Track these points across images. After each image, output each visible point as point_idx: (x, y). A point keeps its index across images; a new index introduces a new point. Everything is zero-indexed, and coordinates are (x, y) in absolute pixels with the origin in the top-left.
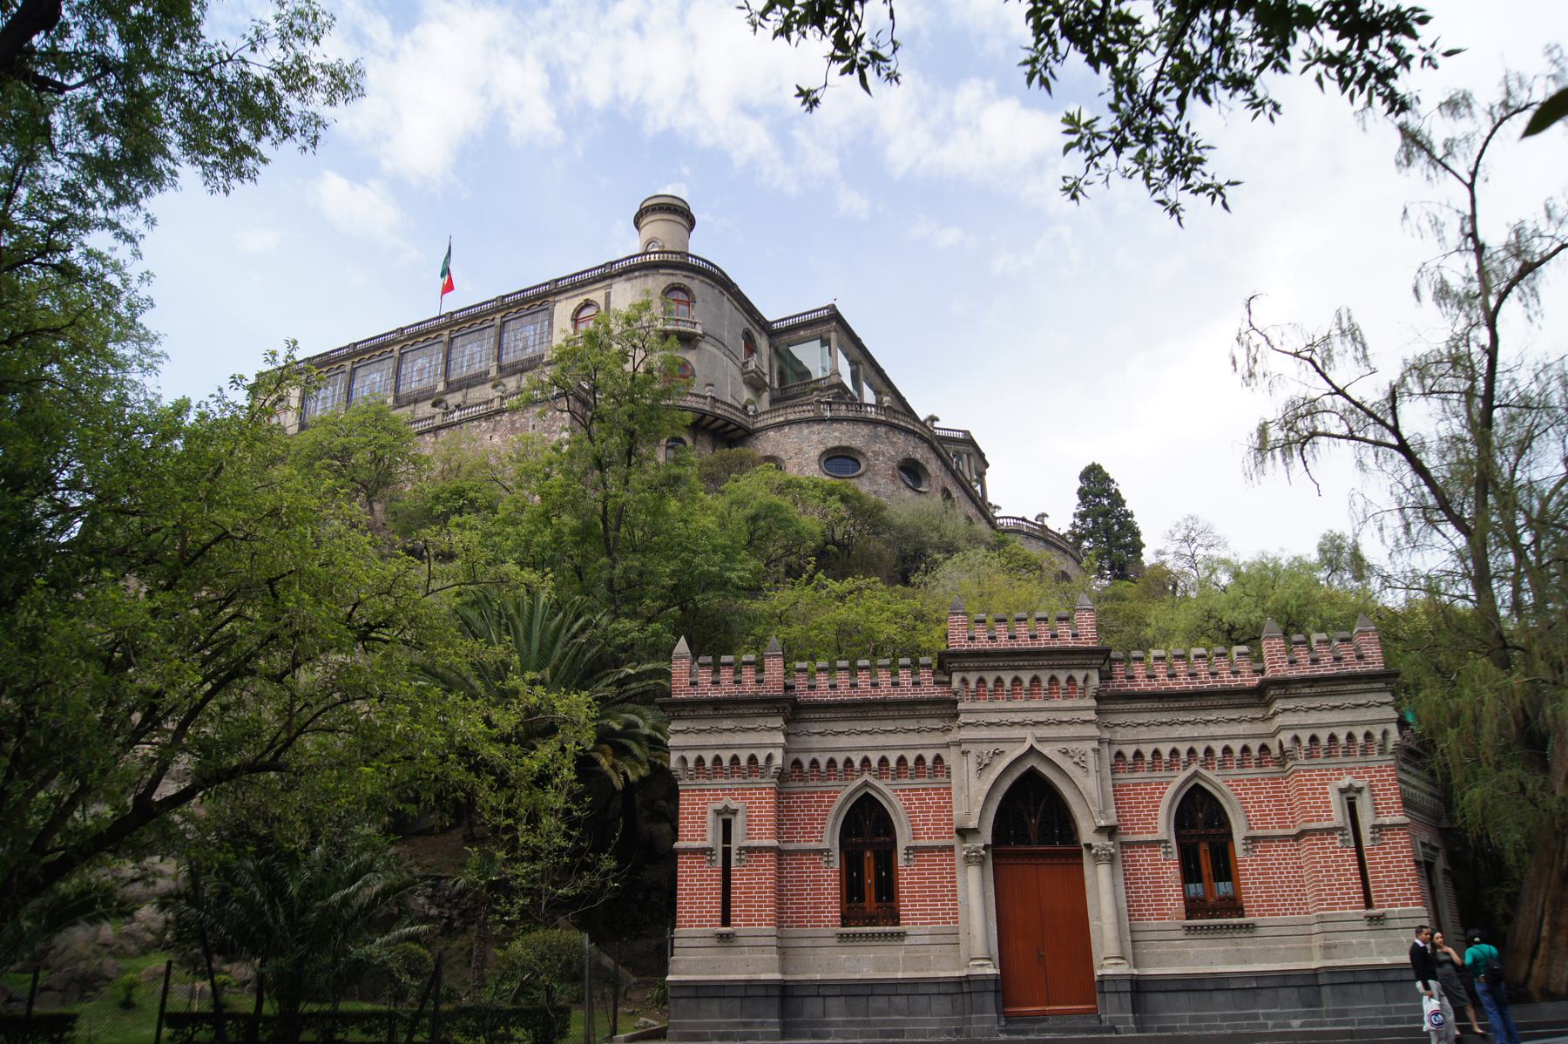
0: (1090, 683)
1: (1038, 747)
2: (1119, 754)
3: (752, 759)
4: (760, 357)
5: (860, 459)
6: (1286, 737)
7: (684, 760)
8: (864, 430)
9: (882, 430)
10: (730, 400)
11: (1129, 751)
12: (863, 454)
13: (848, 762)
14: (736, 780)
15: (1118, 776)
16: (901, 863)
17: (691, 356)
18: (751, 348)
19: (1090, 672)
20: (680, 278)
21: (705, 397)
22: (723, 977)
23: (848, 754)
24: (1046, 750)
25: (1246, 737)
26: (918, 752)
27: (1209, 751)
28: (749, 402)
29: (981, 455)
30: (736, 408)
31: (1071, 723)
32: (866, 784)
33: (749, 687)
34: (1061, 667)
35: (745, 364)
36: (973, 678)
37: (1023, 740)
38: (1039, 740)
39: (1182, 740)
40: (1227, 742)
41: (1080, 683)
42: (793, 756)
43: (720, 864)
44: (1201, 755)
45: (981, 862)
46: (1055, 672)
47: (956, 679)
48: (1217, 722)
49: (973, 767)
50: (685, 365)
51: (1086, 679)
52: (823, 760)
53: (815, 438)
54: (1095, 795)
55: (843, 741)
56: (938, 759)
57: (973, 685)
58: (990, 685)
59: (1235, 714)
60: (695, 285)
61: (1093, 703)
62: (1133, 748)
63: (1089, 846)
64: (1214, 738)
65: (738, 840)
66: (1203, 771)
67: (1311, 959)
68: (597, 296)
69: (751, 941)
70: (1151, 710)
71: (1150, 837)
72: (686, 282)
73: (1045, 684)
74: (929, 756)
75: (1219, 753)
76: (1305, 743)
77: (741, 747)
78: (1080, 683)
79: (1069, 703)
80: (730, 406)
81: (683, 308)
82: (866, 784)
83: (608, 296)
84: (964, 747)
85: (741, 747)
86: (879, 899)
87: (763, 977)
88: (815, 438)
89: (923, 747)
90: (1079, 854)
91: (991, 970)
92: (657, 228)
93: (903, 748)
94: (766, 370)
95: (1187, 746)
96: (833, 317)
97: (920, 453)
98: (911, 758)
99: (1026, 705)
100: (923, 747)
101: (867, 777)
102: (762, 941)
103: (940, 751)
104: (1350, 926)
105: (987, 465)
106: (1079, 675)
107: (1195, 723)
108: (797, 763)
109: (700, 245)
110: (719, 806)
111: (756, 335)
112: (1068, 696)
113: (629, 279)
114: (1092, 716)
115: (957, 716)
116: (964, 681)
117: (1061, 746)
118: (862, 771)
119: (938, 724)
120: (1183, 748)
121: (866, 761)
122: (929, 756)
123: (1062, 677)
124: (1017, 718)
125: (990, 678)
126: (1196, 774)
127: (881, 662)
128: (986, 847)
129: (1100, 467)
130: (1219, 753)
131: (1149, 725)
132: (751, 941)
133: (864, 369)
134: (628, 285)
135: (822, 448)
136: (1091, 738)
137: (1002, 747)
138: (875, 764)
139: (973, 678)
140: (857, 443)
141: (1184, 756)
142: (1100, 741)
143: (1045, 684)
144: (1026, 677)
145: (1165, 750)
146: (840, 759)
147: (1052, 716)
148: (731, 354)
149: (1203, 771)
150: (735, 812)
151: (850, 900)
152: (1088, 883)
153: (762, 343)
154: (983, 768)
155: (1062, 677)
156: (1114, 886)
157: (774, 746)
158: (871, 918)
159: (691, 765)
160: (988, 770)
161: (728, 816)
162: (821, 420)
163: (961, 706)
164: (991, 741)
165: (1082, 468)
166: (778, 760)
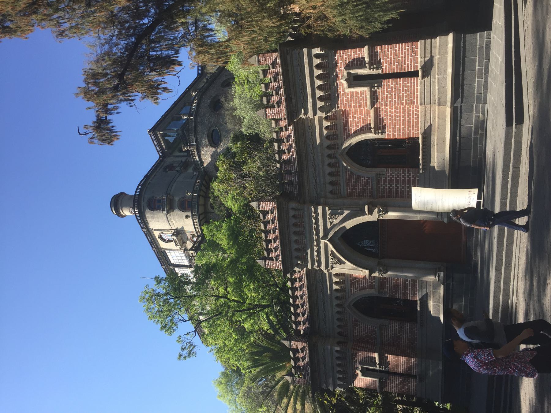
2: (331, 192)
5: (212, 129)
8: (200, 128)
9: (199, 119)
11: (329, 188)
12: (210, 128)
18: (171, 167)
41: (296, 213)
51: (293, 209)
68: (157, 234)
72: (146, 201)
78: (296, 213)
83: (156, 230)
94: (180, 159)
104: (427, 88)
106: (292, 213)
109: (131, 191)
113: (148, 223)
137: (330, 252)
145: (328, 170)
153: (169, 160)
157: (332, 349)
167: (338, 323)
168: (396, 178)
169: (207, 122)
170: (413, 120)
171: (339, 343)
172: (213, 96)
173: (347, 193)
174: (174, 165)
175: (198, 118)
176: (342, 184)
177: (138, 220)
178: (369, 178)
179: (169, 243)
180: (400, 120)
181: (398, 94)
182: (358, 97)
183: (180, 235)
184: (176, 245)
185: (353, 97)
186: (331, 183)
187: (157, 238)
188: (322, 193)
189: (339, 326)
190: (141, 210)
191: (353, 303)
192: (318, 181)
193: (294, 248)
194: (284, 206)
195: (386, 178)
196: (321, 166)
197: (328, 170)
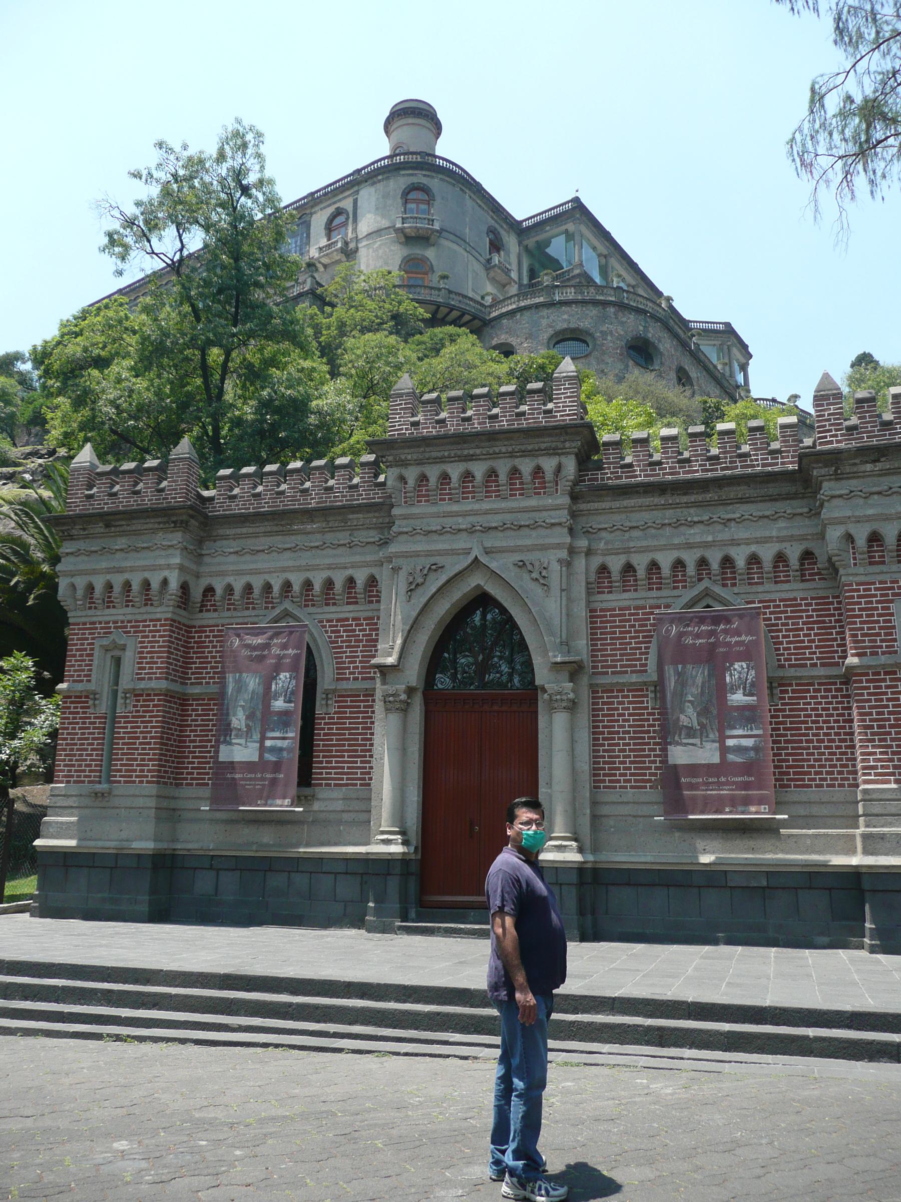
0: (563, 473)
1: (483, 559)
2: (603, 569)
4: (508, 254)
5: (588, 339)
6: (834, 534)
7: (73, 587)
8: (593, 311)
11: (616, 564)
12: (591, 335)
15: (592, 598)
17: (430, 253)
18: (496, 246)
19: (563, 459)
20: (420, 178)
21: (439, 289)
22: (92, 844)
23: (267, 577)
24: (493, 565)
25: (780, 540)
27: (727, 562)
28: (487, 294)
29: (745, 347)
31: (534, 526)
34: (525, 454)
35: (489, 261)
36: (411, 474)
37: (468, 551)
38: (487, 552)
39: (689, 546)
40: (753, 548)
41: (549, 476)
45: (405, 709)
46: (517, 462)
49: (403, 587)
50: (424, 260)
51: (559, 469)
53: (544, 322)
54: (556, 622)
55: (262, 562)
56: (372, 582)
57: (411, 482)
59: (767, 509)
60: (435, 183)
61: (566, 500)
64: (734, 543)
65: (125, 682)
67: (852, 851)
70: (650, 508)
71: (634, 678)
72: (425, 181)
75: (741, 563)
76: (861, 541)
77: (132, 569)
78: (549, 476)
79: (533, 502)
80: (471, 299)
81: (423, 207)
83: (355, 202)
84: (396, 562)
85: (132, 569)
87: (135, 845)
88: (544, 322)
92: (407, 132)
93: (330, 567)
94: (514, 266)
95: (697, 554)
96: (577, 210)
97: (654, 332)
98: (339, 580)
99: (476, 507)
100: (354, 566)
101: (287, 605)
105: (751, 356)
106: (549, 464)
107: (710, 523)
109: (446, 148)
110: (105, 642)
111: (503, 233)
113: (374, 184)
114: (563, 516)
116: (402, 479)
120: (690, 558)
121: (287, 586)
122: (361, 577)
123: (526, 466)
124: (463, 523)
125: (433, 473)
126: (707, 593)
128: (410, 691)
129: (870, 355)
131: (645, 528)
133: (614, 262)
134: (372, 190)
135: (551, 331)
136: (558, 546)
137: (440, 560)
139: (411, 474)
140: (585, 324)
141: (691, 570)
142: (572, 551)
144: (479, 470)
145: (665, 560)
149: (717, 589)
152: (541, 736)
153: (511, 241)
154: (413, 588)
155: (526, 466)
156: (573, 741)
157: (169, 567)
160: (420, 590)
161: (117, 653)
162: (551, 305)
163: (395, 511)
164: (429, 554)
165: (853, 358)
167: (238, 586)
168: (649, 732)
169: (604, 329)
170: (810, 773)
171: (184, 588)
172: (661, 347)
173: (602, 610)
174: (502, 253)
175: (612, 310)
176: (626, 595)
177: (376, 162)
178: (646, 665)
179: (323, 232)
180: (807, 741)
181: (890, 733)
182: (879, 635)
183: (344, 259)
184: (321, 249)
185: (878, 622)
186: (629, 568)
187: (336, 206)
188: (602, 545)
189: (229, 589)
190: (404, 169)
192: (636, 533)
193: (449, 471)
194: (567, 445)
195: (647, 708)
196: (676, 541)
197: (665, 560)
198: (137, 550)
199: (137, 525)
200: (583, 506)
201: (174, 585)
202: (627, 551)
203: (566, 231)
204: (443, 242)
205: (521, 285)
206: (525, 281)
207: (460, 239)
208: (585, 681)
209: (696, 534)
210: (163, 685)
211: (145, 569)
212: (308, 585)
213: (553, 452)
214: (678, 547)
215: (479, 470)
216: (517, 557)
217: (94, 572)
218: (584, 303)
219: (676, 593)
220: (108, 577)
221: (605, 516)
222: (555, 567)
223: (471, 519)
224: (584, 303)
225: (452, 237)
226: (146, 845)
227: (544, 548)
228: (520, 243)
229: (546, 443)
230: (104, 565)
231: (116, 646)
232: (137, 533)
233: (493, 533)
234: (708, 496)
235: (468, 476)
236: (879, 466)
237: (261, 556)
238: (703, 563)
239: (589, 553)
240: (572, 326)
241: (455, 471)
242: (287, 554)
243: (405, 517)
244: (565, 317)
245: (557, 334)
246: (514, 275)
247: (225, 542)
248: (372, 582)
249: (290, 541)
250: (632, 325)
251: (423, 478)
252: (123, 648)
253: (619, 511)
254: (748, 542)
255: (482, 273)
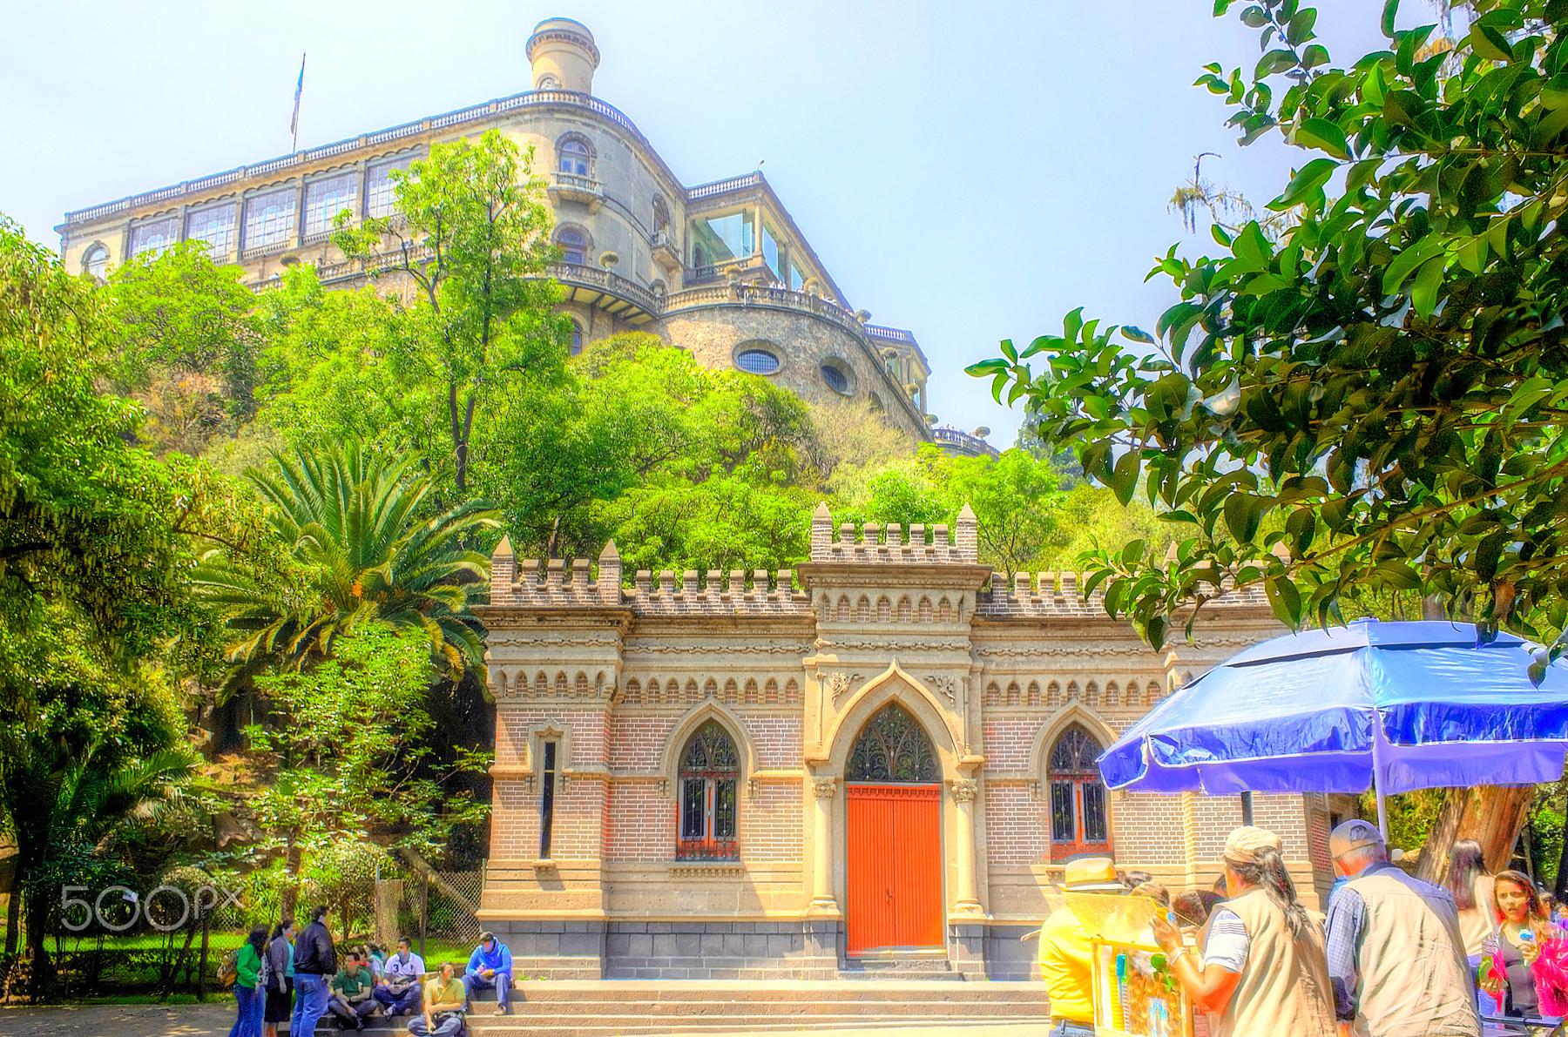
0: (966, 605)
1: (902, 673)
2: (993, 685)
3: (582, 677)
5: (778, 354)
8: (785, 322)
9: (805, 322)
10: (634, 279)
11: (1004, 682)
12: (782, 350)
13: (692, 685)
14: (562, 700)
15: (989, 709)
16: (743, 793)
17: (588, 223)
18: (663, 218)
19: (966, 593)
21: (604, 273)
23: (692, 675)
24: (910, 678)
25: (1134, 672)
26: (771, 675)
27: (1092, 686)
30: (641, 289)
31: (942, 649)
32: (710, 708)
33: (582, 598)
34: (935, 587)
35: (654, 238)
36: (834, 595)
39: (1064, 672)
40: (1112, 677)
42: (630, 675)
43: (541, 792)
44: (1083, 690)
46: (927, 593)
47: (817, 593)
48: (1103, 654)
52: (663, 681)
55: (687, 661)
58: (854, 603)
61: (967, 629)
62: (1010, 679)
63: (951, 783)
64: (1099, 672)
66: (1083, 707)
69: (574, 875)
70: (1032, 639)
73: (915, 605)
74: (782, 680)
75: (1102, 688)
79: (940, 628)
82: (710, 708)
86: (718, 833)
89: (775, 670)
90: (938, 792)
91: (833, 912)
93: (753, 670)
94: (679, 246)
99: (892, 628)
101: (711, 701)
102: (584, 875)
103: (795, 675)
106: (954, 597)
107: (1080, 654)
108: (634, 683)
110: (541, 728)
112: (940, 619)
114: (965, 643)
115: (815, 636)
116: (825, 598)
117: (928, 673)
118: (707, 695)
119: (793, 645)
120: (1063, 682)
121: (711, 683)
122: (782, 680)
125: (854, 596)
127: (733, 573)
130: (1102, 688)
132: (574, 875)
136: (962, 666)
138: (721, 686)
139: (834, 595)
140: (777, 336)
141: (1064, 691)
143: (915, 605)
145: (1044, 682)
146: (683, 681)
147: (920, 640)
148: (637, 223)
150: (560, 735)
151: (687, 833)
154: (839, 696)
157: (606, 662)
158: (709, 852)
159: (511, 681)
161: (552, 740)
166: (610, 679)
176: (1010, 709)
188: (993, 666)
191: (717, 718)
192: (1019, 658)
197: (1044, 682)
198: (571, 645)
199: (571, 621)
200: (979, 633)
201: (610, 679)
202: (1014, 673)
203: (744, 211)
204: (605, 211)
205: (686, 269)
206: (691, 266)
207: (625, 208)
208: (983, 777)
209: (1069, 664)
210: (603, 770)
211: (580, 662)
212: (731, 684)
213: (959, 588)
214: (1055, 672)
215: (895, 596)
216: (928, 673)
217: (526, 663)
218: (775, 310)
219: (1051, 708)
220: (542, 668)
221: (1001, 642)
222: (959, 681)
223: (886, 638)
224: (775, 310)
225: (615, 206)
226: (598, 912)
227: (950, 667)
228: (686, 216)
229: (954, 579)
230: (537, 656)
231: (550, 732)
232: (570, 628)
233: (906, 652)
234: (1080, 633)
235: (884, 600)
236: (1214, 623)
237: (685, 655)
238: (1072, 686)
239: (983, 672)
240: (763, 337)
241: (874, 596)
242: (712, 655)
243: (828, 632)
244: (754, 324)
245: (743, 344)
246: (681, 257)
247: (647, 640)
248: (792, 683)
249: (715, 644)
250: (828, 342)
251: (844, 599)
252: (560, 735)
253: (1008, 639)
254: (1109, 672)
255: (647, 252)
